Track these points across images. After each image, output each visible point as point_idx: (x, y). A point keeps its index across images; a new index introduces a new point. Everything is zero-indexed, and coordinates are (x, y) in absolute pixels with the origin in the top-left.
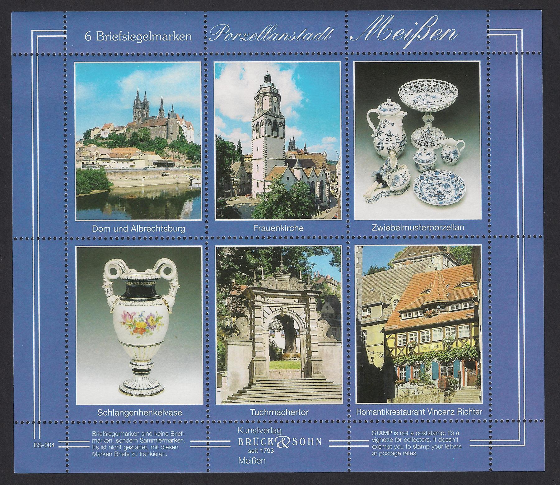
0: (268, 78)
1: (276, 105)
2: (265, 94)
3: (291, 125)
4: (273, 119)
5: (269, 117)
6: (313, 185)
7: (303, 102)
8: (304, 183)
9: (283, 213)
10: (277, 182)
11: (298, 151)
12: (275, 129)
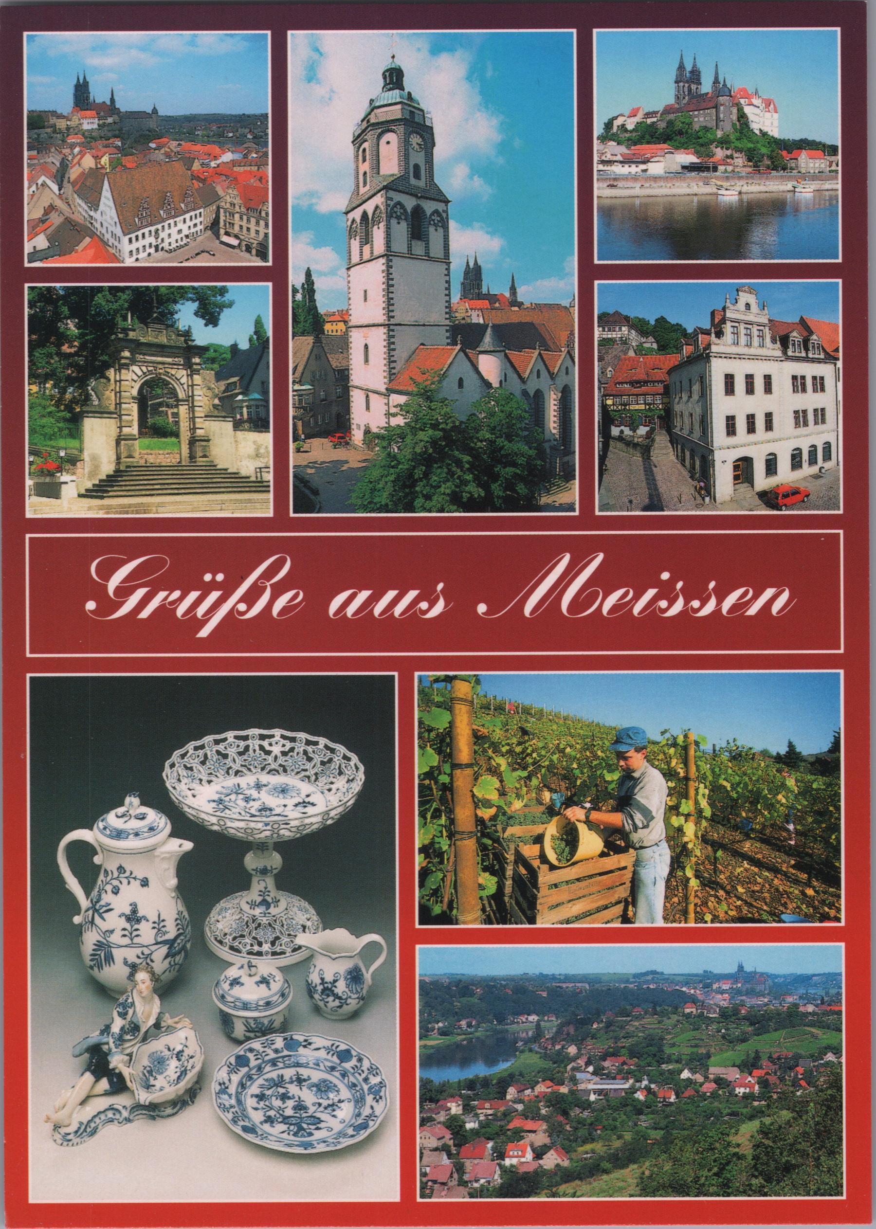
0: (394, 78)
1: (418, 158)
2: (386, 127)
3: (467, 223)
4: (410, 203)
5: (398, 197)
6: (537, 400)
7: (503, 148)
8: (510, 397)
9: (447, 488)
10: (427, 395)
11: (492, 298)
12: (417, 233)
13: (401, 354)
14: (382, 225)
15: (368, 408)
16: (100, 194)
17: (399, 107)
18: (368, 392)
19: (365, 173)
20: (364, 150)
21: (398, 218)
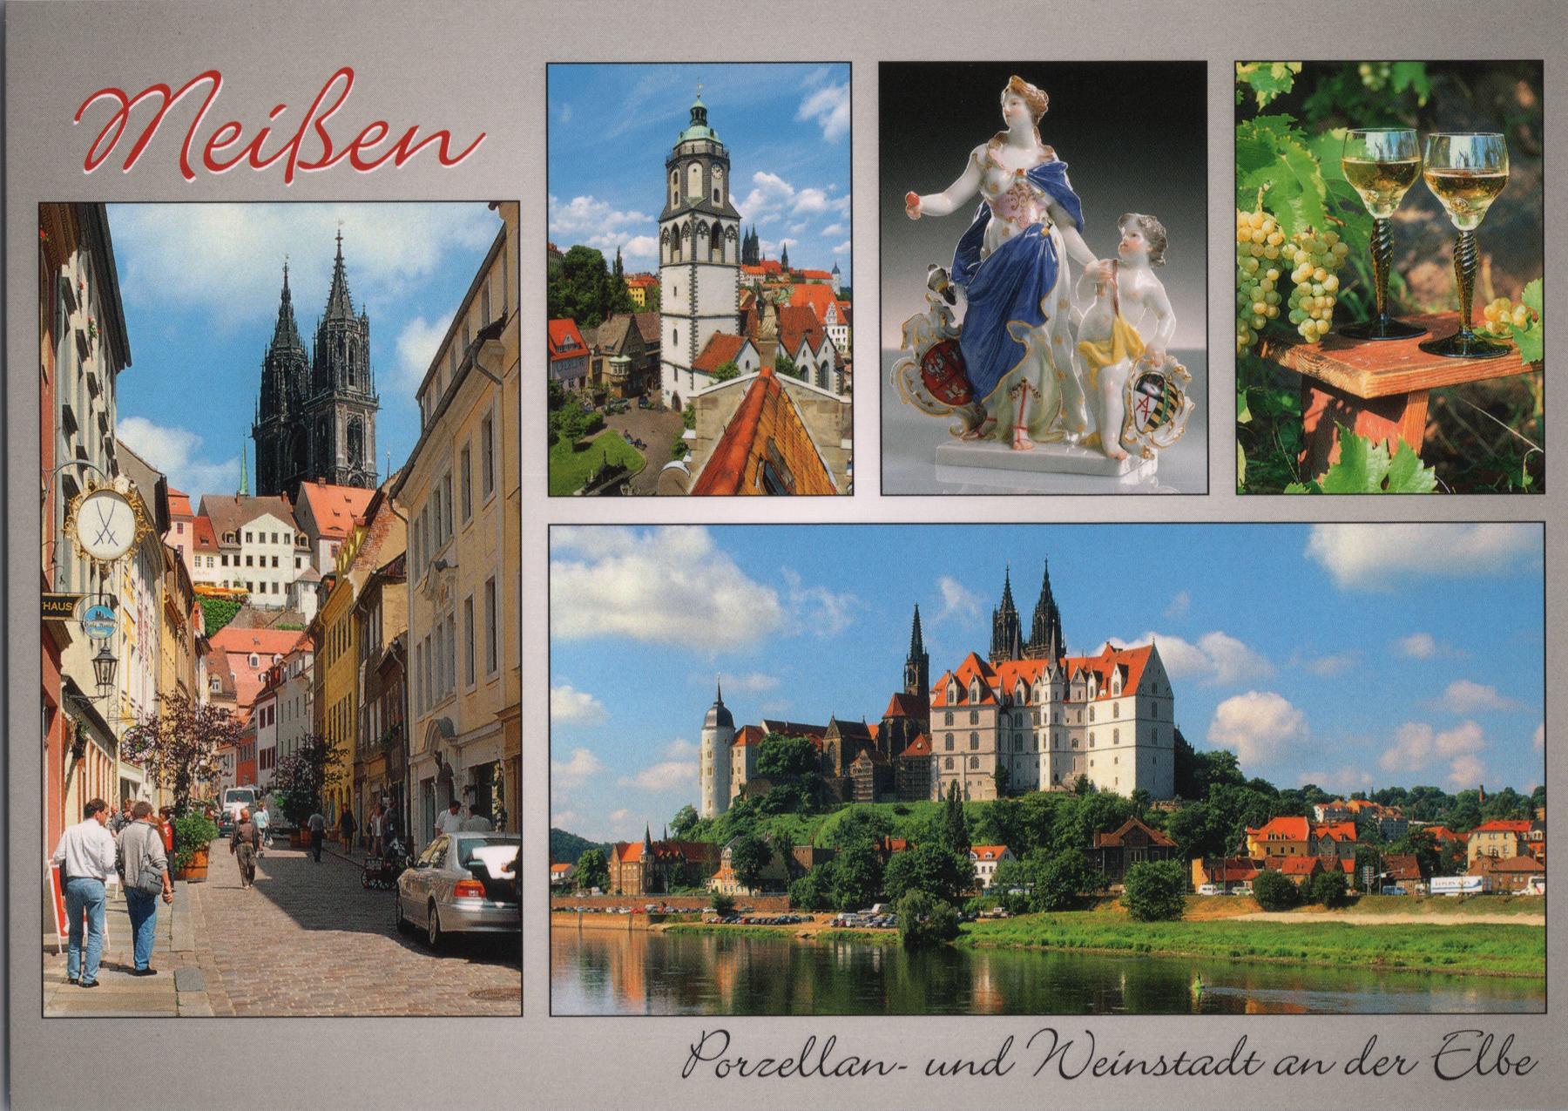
2: (694, 157)
4: (711, 221)
5: (701, 217)
13: (702, 342)
18: (676, 367)
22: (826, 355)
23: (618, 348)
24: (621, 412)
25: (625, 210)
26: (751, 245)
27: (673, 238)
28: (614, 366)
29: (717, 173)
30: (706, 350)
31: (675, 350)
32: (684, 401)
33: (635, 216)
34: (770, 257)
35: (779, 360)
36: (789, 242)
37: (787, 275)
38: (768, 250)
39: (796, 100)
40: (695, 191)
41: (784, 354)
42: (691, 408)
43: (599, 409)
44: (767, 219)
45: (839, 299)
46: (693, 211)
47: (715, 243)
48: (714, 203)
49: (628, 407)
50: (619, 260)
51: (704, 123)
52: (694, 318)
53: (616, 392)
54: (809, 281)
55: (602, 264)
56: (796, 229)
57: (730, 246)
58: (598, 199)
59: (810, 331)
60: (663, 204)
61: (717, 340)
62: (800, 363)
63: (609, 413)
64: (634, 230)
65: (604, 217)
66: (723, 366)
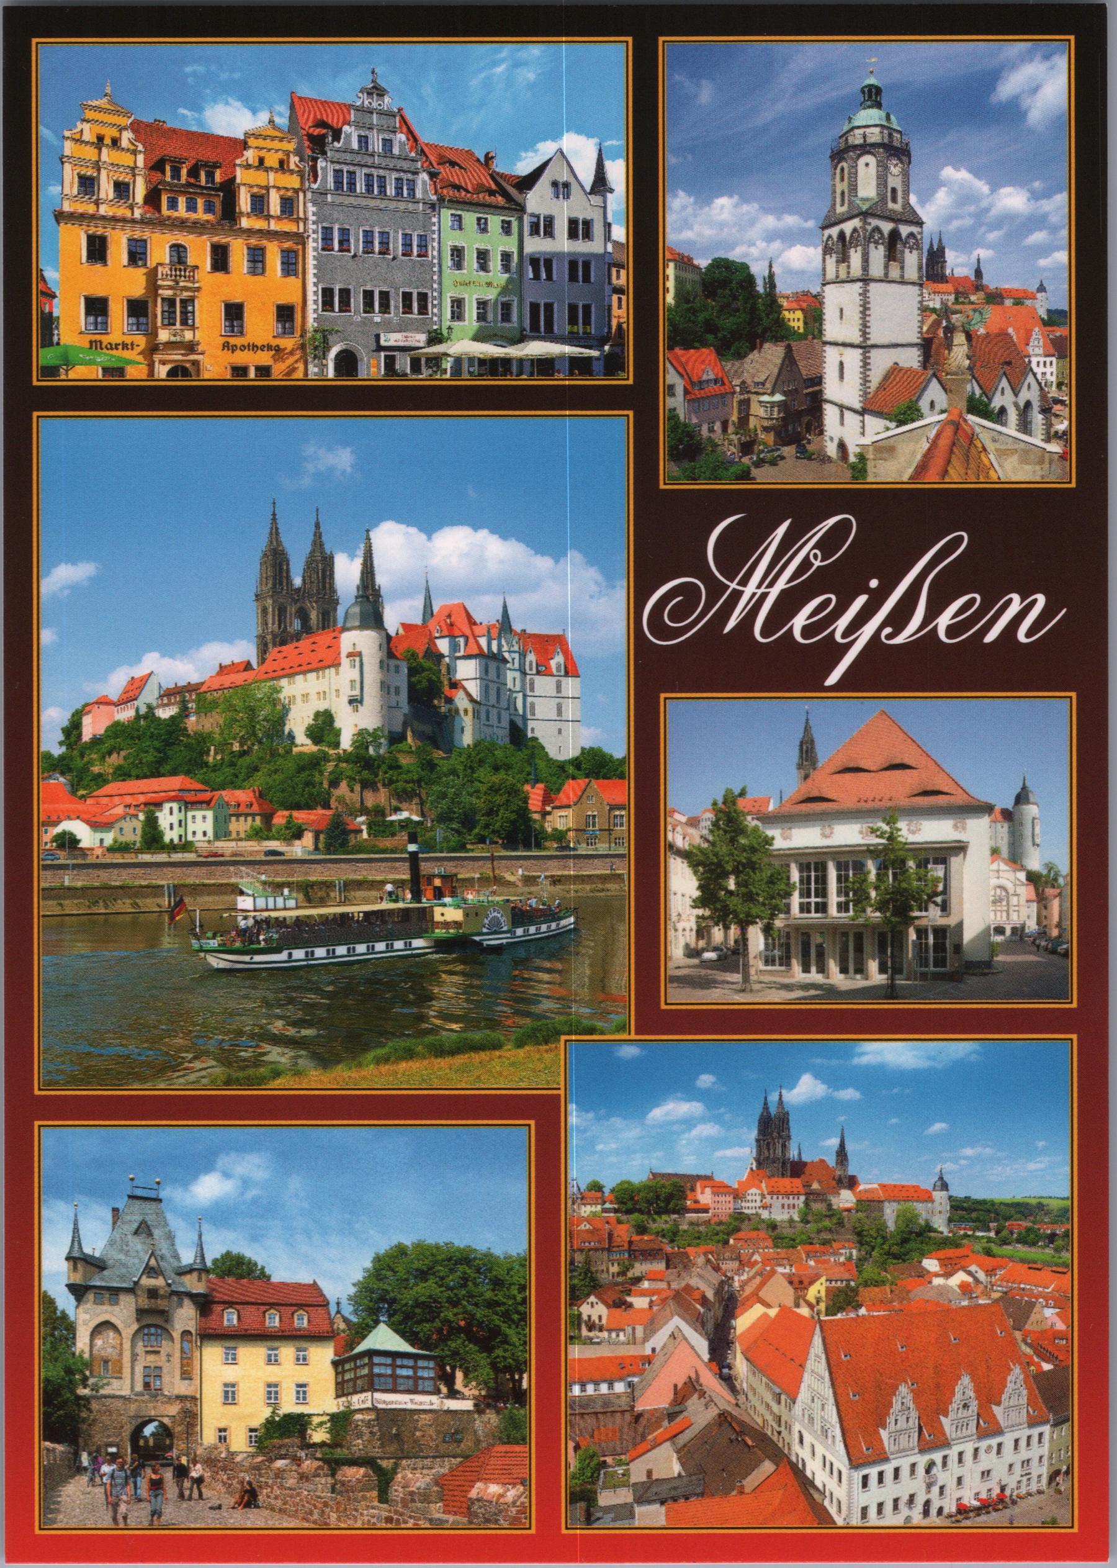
2: (866, 148)
4: (887, 227)
13: (876, 377)
14: (859, 249)
15: (842, 424)
16: (802, 1366)
17: (877, 130)
18: (842, 408)
19: (843, 193)
20: (842, 170)
21: (876, 243)
22: (1030, 394)
23: (769, 385)
24: (773, 463)
25: (778, 212)
26: (936, 257)
27: (840, 248)
28: (764, 407)
29: (895, 169)
30: (882, 386)
31: (842, 386)
32: (852, 450)
33: (791, 220)
34: (960, 272)
35: (971, 399)
36: (984, 253)
37: (981, 294)
38: (957, 264)
39: (992, 78)
40: (868, 189)
41: (978, 392)
42: (862, 457)
43: (746, 460)
44: (956, 224)
45: (1046, 323)
46: (865, 215)
47: (892, 255)
48: (891, 205)
49: (783, 458)
50: (771, 276)
51: (879, 105)
52: (865, 347)
53: (770, 438)
54: (1008, 302)
55: (750, 280)
56: (992, 236)
57: (912, 259)
58: (745, 200)
59: (1009, 363)
60: (829, 204)
61: (895, 370)
62: (997, 403)
63: (759, 464)
64: (790, 237)
65: (752, 223)
66: (903, 404)
